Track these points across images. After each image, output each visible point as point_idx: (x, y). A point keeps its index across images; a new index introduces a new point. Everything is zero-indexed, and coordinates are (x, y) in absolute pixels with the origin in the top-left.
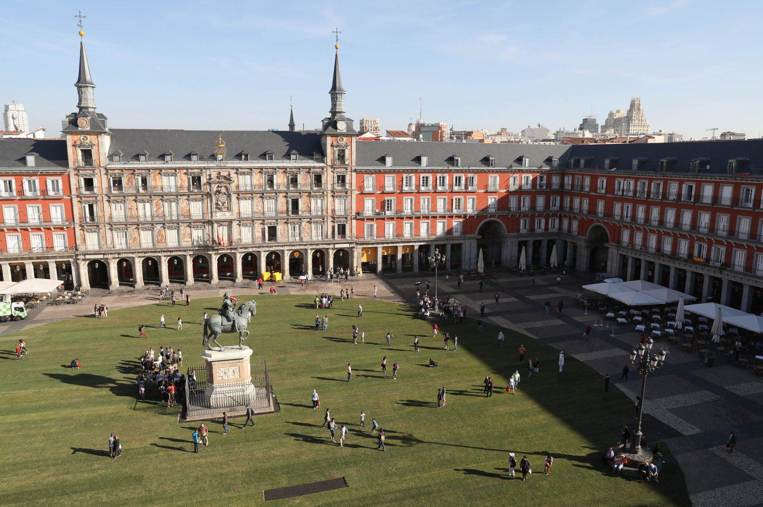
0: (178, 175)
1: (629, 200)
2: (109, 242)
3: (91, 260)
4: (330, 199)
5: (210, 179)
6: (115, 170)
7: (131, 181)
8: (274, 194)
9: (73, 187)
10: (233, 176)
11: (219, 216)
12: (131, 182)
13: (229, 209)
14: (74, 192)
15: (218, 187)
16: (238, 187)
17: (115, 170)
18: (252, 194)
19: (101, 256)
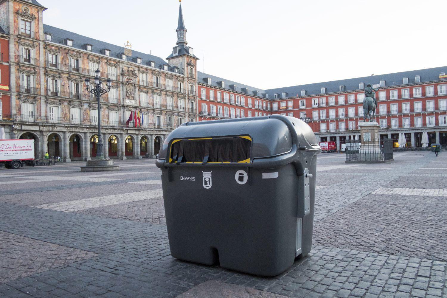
0: (101, 63)
1: (323, 108)
2: (43, 114)
3: (25, 132)
4: (187, 101)
5: (123, 71)
6: (53, 46)
7: (65, 60)
8: (159, 91)
9: (12, 54)
10: (136, 72)
11: (128, 102)
12: (65, 61)
13: (134, 98)
14: (12, 59)
15: (127, 79)
16: (139, 82)
17: (53, 46)
18: (147, 89)
19: (37, 128)
